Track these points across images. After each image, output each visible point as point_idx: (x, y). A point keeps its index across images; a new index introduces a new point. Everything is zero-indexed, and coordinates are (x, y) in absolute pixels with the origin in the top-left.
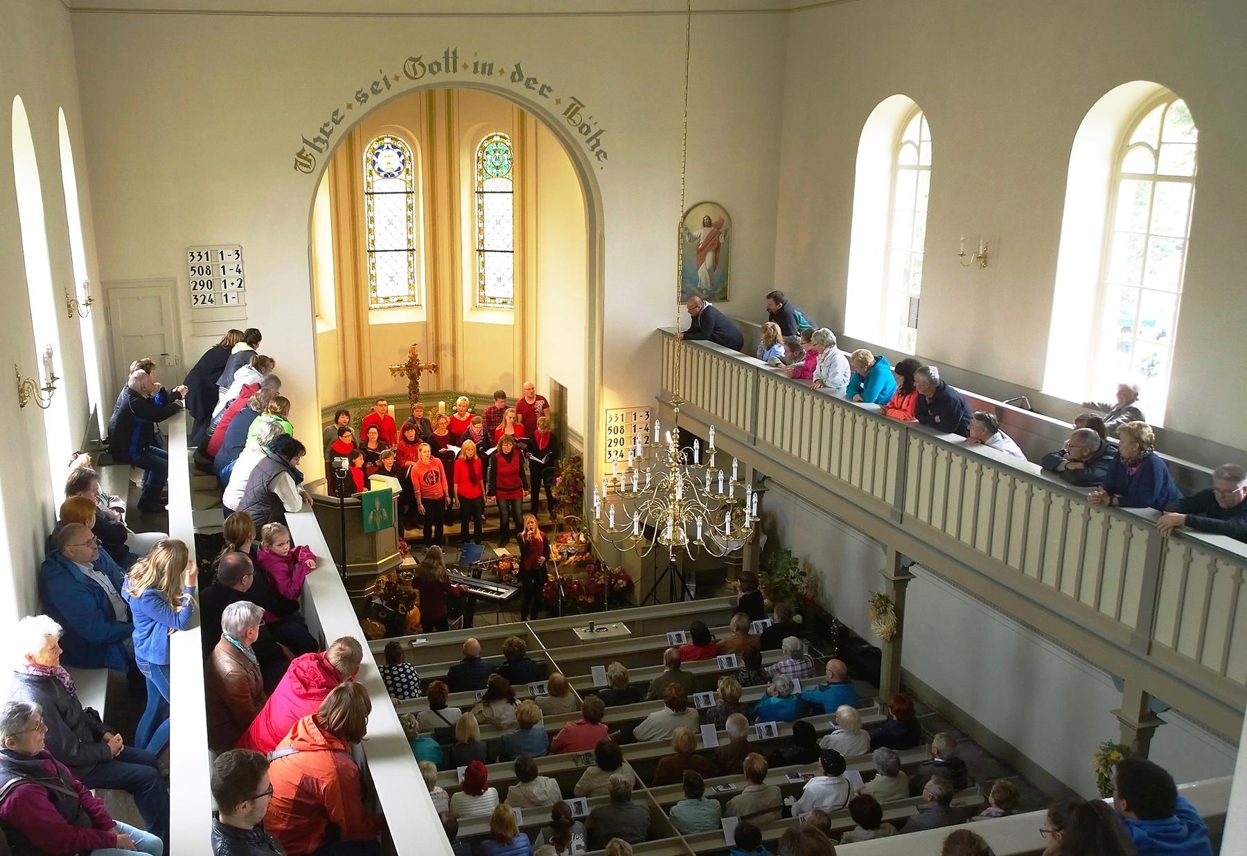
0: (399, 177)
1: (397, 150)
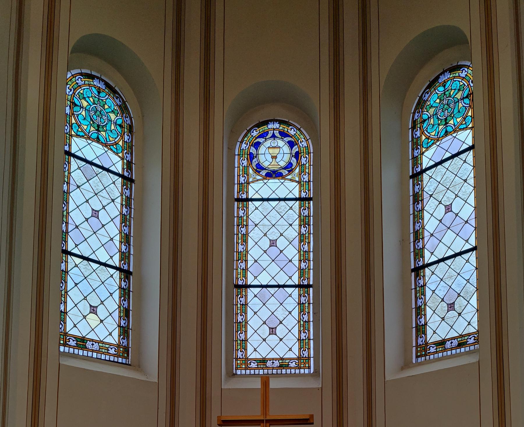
1: (289, 139)
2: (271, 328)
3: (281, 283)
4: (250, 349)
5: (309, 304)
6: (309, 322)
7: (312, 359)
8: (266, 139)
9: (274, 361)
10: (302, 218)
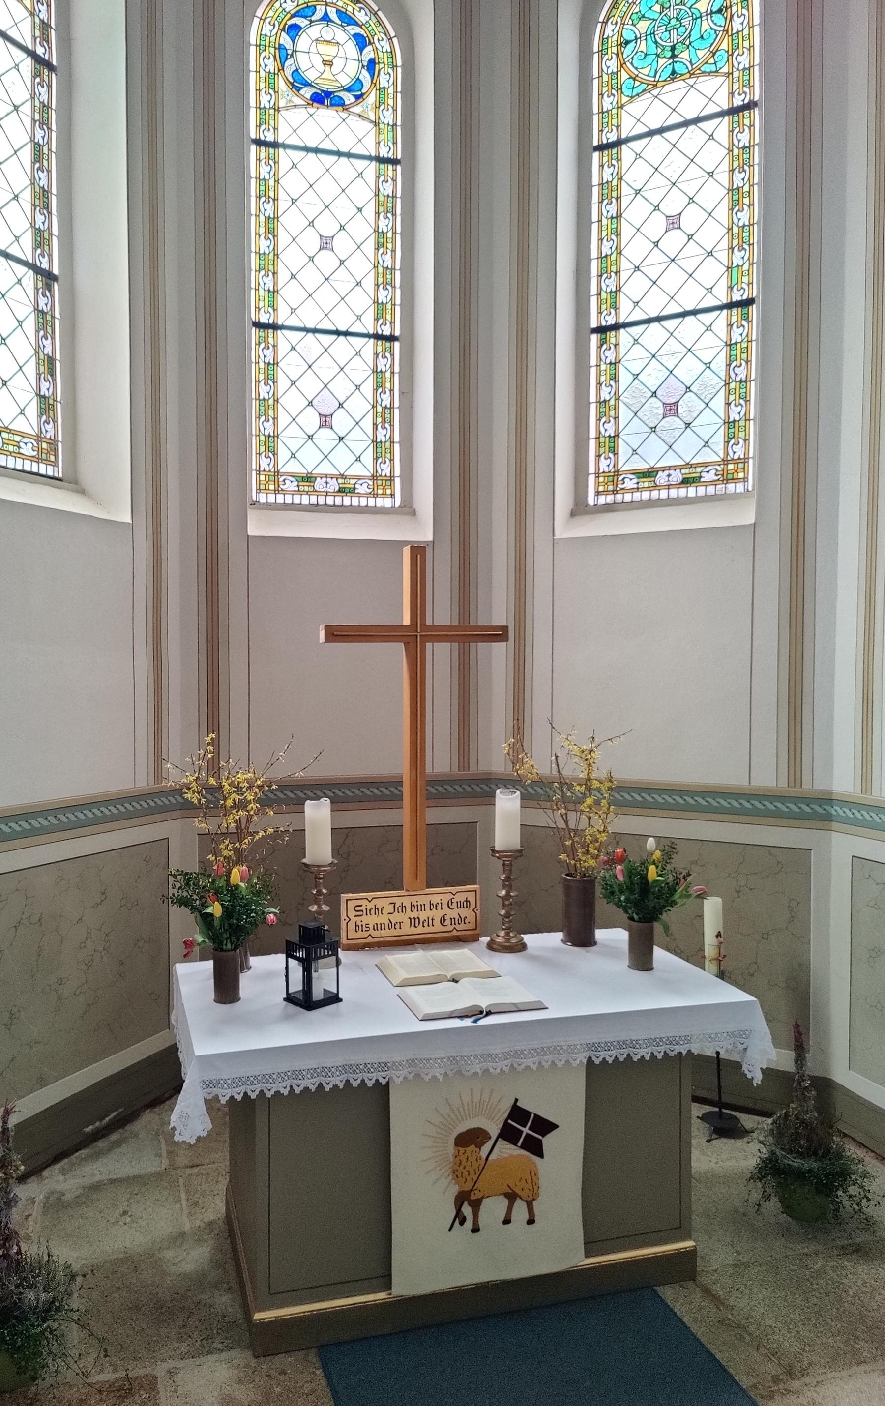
0: (357, 109)
1: (358, 30)
2: (323, 415)
3: (342, 328)
4: (283, 454)
5: (393, 373)
6: (391, 408)
7: (397, 481)
8: (311, 22)
9: (329, 480)
10: (381, 198)
